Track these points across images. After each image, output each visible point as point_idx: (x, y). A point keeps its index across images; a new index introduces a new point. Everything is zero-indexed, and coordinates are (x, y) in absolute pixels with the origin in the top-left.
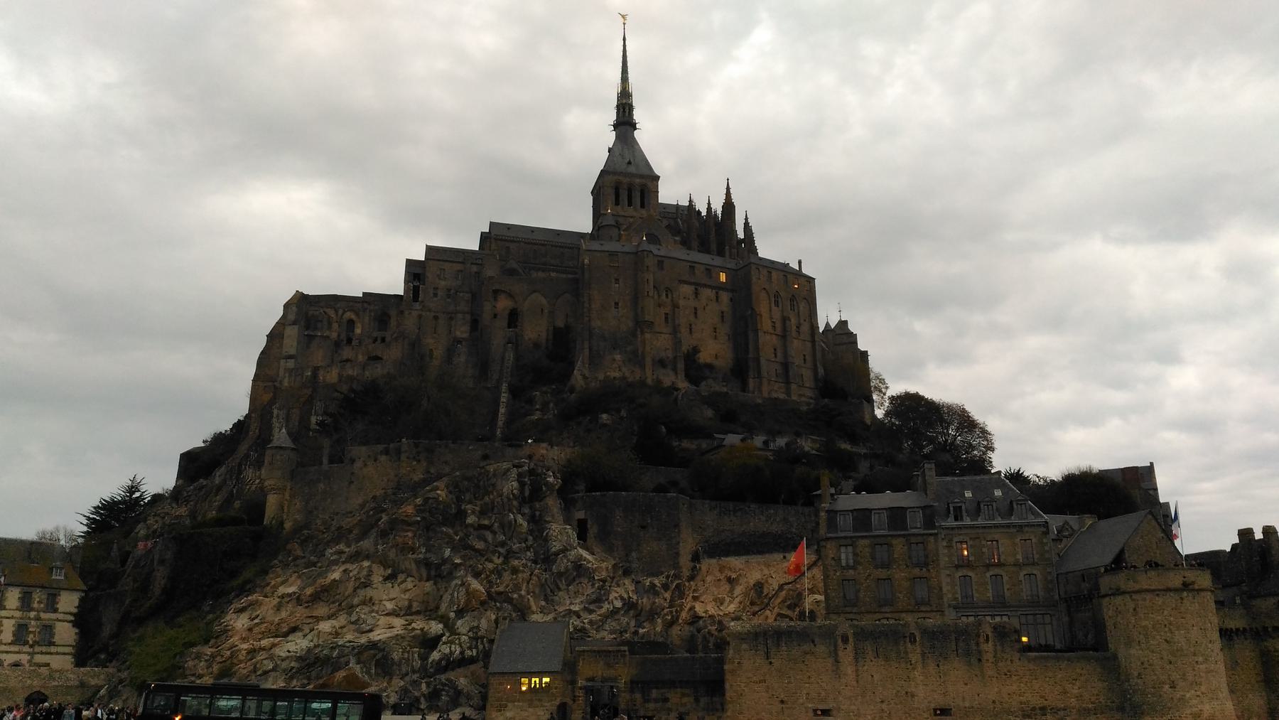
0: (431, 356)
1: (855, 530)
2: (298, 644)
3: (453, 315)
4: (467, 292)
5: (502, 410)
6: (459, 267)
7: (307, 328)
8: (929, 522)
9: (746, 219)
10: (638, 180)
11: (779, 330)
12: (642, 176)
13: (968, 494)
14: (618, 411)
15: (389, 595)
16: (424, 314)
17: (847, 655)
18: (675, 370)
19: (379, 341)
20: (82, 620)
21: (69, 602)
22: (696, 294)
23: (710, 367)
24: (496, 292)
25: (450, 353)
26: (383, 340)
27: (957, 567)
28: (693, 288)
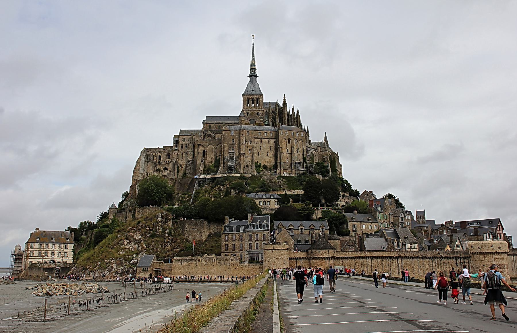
1: (229, 232)
3: (188, 153)
4: (192, 145)
6: (190, 137)
8: (244, 230)
9: (293, 107)
10: (255, 97)
11: (289, 152)
12: (257, 95)
13: (259, 221)
16: (178, 153)
17: (199, 264)
19: (167, 162)
21: (71, 247)
22: (261, 142)
24: (199, 145)
25: (186, 166)
27: (249, 241)
28: (260, 139)
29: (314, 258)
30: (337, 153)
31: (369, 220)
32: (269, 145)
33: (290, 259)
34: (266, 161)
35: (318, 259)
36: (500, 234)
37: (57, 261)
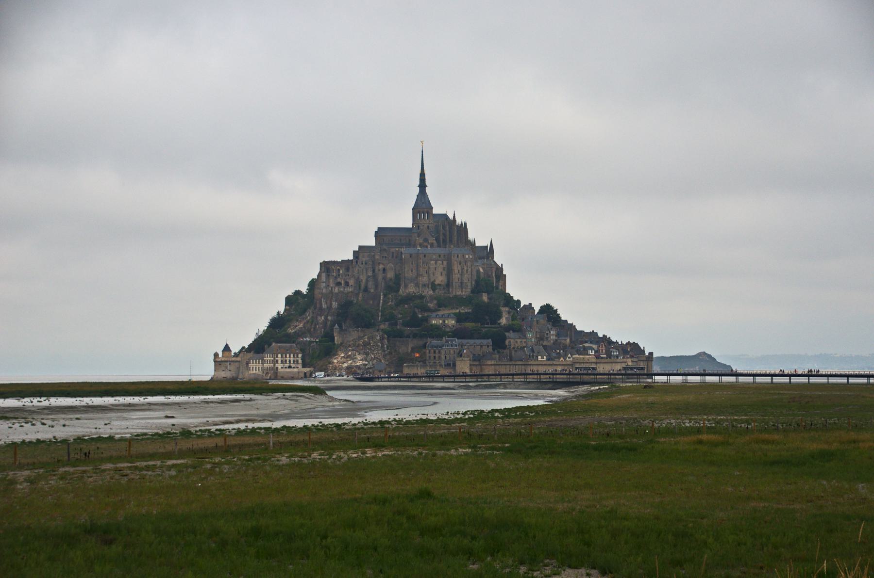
0: (362, 281)
2: (345, 365)
5: (381, 302)
6: (369, 253)
7: (327, 272)
9: (462, 222)
10: (425, 210)
11: (460, 273)
14: (410, 304)
15: (359, 357)
17: (419, 368)
18: (428, 287)
20: (302, 359)
21: (300, 356)
22: (436, 263)
23: (439, 285)
24: (379, 263)
25: (367, 281)
26: (348, 275)
29: (483, 365)
30: (502, 265)
31: (520, 337)
32: (441, 266)
33: (470, 365)
34: (440, 280)
35: (486, 365)
36: (602, 350)
37: (293, 366)
